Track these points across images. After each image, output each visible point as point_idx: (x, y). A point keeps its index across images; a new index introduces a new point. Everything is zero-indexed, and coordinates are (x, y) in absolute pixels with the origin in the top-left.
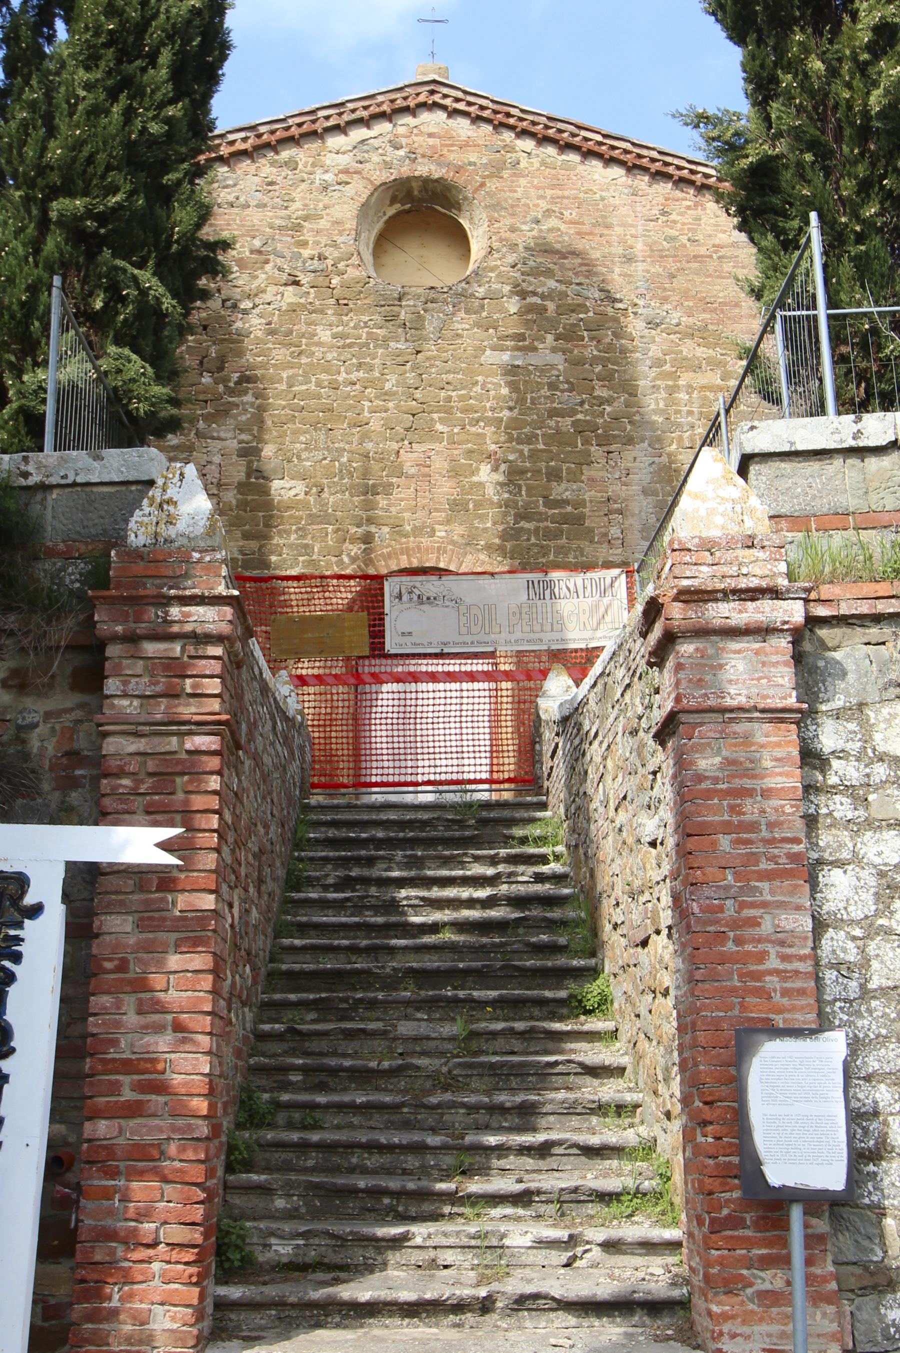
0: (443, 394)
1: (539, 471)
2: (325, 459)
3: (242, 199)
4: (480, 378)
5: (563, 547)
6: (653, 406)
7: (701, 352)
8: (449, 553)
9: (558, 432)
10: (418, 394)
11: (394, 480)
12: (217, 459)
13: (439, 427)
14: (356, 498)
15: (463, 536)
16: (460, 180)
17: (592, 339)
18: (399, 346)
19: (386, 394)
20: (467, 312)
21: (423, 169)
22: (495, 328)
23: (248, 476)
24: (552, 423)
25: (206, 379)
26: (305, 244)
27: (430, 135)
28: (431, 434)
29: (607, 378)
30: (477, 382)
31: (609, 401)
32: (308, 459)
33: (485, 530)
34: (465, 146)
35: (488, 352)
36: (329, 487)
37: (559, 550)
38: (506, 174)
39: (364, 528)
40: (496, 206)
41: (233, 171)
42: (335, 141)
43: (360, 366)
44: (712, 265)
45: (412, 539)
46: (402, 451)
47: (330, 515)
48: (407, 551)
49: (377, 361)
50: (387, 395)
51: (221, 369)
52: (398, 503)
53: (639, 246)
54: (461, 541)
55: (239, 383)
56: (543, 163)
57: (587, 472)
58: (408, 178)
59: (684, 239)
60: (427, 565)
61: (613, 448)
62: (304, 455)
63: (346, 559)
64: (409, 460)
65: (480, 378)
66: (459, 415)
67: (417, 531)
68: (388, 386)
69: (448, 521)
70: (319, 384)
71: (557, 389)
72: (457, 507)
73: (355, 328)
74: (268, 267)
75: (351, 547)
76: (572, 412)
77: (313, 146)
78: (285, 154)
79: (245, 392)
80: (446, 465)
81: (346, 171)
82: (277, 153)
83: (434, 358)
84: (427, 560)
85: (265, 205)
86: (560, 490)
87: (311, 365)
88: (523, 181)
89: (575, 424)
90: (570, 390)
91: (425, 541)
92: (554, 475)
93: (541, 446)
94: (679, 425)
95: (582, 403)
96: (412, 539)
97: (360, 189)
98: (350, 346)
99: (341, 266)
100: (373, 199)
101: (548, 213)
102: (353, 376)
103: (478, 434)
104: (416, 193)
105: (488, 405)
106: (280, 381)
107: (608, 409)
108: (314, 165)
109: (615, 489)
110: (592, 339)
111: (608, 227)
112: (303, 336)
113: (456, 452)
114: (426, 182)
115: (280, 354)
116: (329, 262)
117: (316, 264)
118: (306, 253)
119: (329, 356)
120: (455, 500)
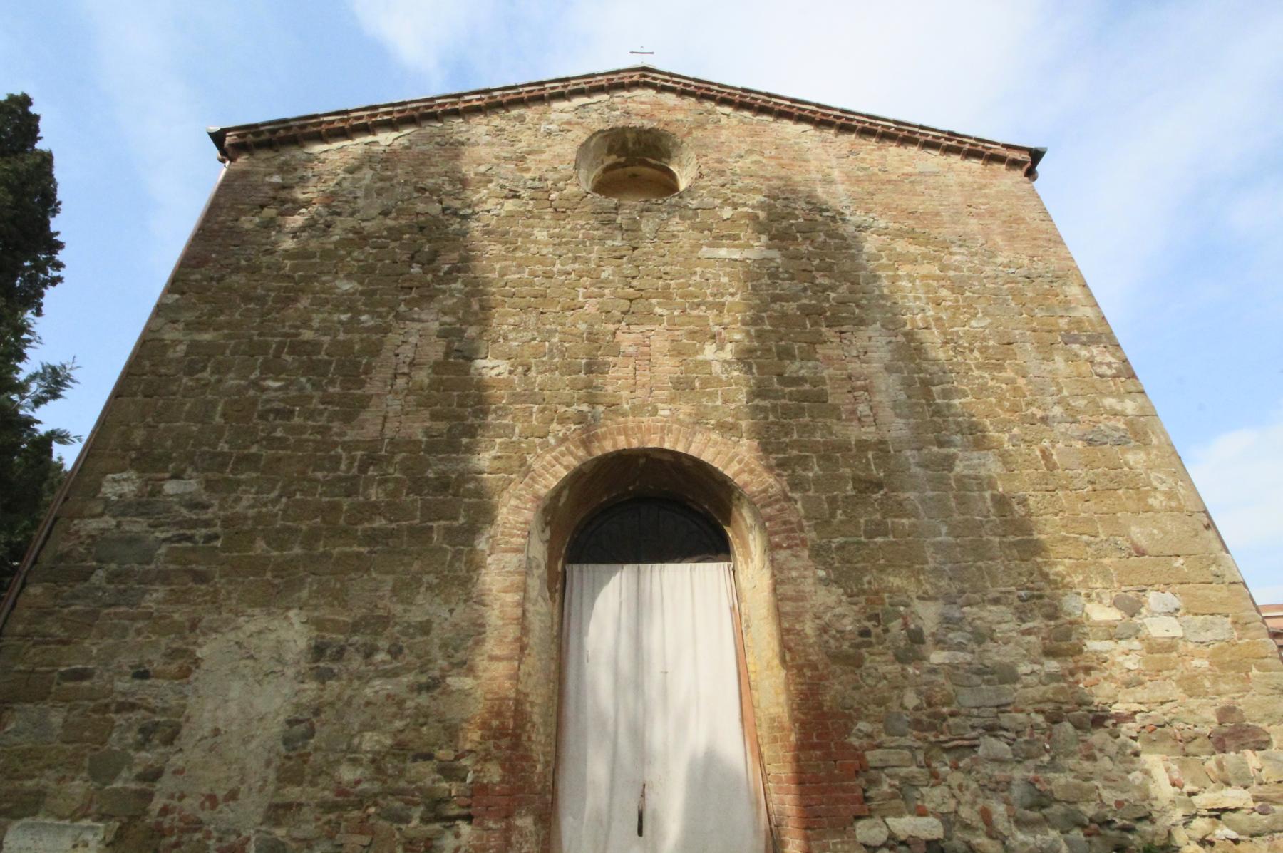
0: (661, 283)
1: (769, 350)
2: (534, 339)
3: (472, 140)
4: (698, 269)
5: (807, 425)
6: (877, 292)
7: (913, 249)
8: (675, 432)
9: (784, 315)
10: (635, 283)
11: (611, 359)
13: (658, 310)
14: (566, 377)
15: (690, 415)
16: (671, 129)
17: (805, 239)
18: (616, 243)
19: (602, 282)
20: (682, 218)
21: (636, 122)
22: (710, 230)
23: (447, 355)
24: (777, 306)
25: (416, 269)
26: (528, 170)
27: (642, 103)
28: (650, 316)
29: (827, 269)
30: (695, 273)
31: (832, 288)
32: (515, 340)
33: (715, 408)
34: (674, 108)
35: (705, 248)
36: (537, 366)
37: (803, 428)
38: (709, 127)
39: (575, 407)
40: (704, 146)
41: (467, 122)
42: (557, 105)
43: (575, 259)
44: (906, 187)
45: (631, 418)
46: (618, 332)
47: (536, 394)
48: (624, 431)
50: (601, 284)
51: (431, 261)
52: (617, 380)
53: (836, 174)
54: (688, 420)
55: (449, 273)
56: (741, 121)
57: (821, 351)
58: (623, 128)
59: (875, 170)
60: (650, 446)
61: (845, 328)
62: (511, 336)
63: (552, 440)
64: (627, 340)
65: (698, 269)
66: (678, 300)
67: (636, 410)
68: (604, 275)
69: (672, 400)
71: (778, 278)
72: (682, 386)
73: (571, 229)
74: (490, 185)
75: (559, 427)
76: (794, 298)
77: (540, 108)
78: (515, 112)
80: (667, 344)
81: (569, 123)
82: (508, 111)
83: (652, 253)
84: (650, 441)
85: (493, 144)
86: (794, 368)
87: (526, 258)
88: (724, 132)
89: (799, 308)
90: (792, 279)
92: (786, 354)
94: (908, 309)
95: (805, 289)
96: (631, 418)
97: (580, 135)
98: (566, 243)
99: (561, 184)
100: (592, 144)
101: (750, 152)
102: (569, 268)
103: (700, 317)
104: (630, 145)
105: (708, 292)
106: (493, 270)
107: (832, 295)
110: (805, 239)
111: (807, 161)
112: (520, 235)
113: (677, 333)
114: (640, 132)
115: (496, 249)
116: (549, 183)
117: (537, 184)
119: (544, 251)
120: (678, 378)
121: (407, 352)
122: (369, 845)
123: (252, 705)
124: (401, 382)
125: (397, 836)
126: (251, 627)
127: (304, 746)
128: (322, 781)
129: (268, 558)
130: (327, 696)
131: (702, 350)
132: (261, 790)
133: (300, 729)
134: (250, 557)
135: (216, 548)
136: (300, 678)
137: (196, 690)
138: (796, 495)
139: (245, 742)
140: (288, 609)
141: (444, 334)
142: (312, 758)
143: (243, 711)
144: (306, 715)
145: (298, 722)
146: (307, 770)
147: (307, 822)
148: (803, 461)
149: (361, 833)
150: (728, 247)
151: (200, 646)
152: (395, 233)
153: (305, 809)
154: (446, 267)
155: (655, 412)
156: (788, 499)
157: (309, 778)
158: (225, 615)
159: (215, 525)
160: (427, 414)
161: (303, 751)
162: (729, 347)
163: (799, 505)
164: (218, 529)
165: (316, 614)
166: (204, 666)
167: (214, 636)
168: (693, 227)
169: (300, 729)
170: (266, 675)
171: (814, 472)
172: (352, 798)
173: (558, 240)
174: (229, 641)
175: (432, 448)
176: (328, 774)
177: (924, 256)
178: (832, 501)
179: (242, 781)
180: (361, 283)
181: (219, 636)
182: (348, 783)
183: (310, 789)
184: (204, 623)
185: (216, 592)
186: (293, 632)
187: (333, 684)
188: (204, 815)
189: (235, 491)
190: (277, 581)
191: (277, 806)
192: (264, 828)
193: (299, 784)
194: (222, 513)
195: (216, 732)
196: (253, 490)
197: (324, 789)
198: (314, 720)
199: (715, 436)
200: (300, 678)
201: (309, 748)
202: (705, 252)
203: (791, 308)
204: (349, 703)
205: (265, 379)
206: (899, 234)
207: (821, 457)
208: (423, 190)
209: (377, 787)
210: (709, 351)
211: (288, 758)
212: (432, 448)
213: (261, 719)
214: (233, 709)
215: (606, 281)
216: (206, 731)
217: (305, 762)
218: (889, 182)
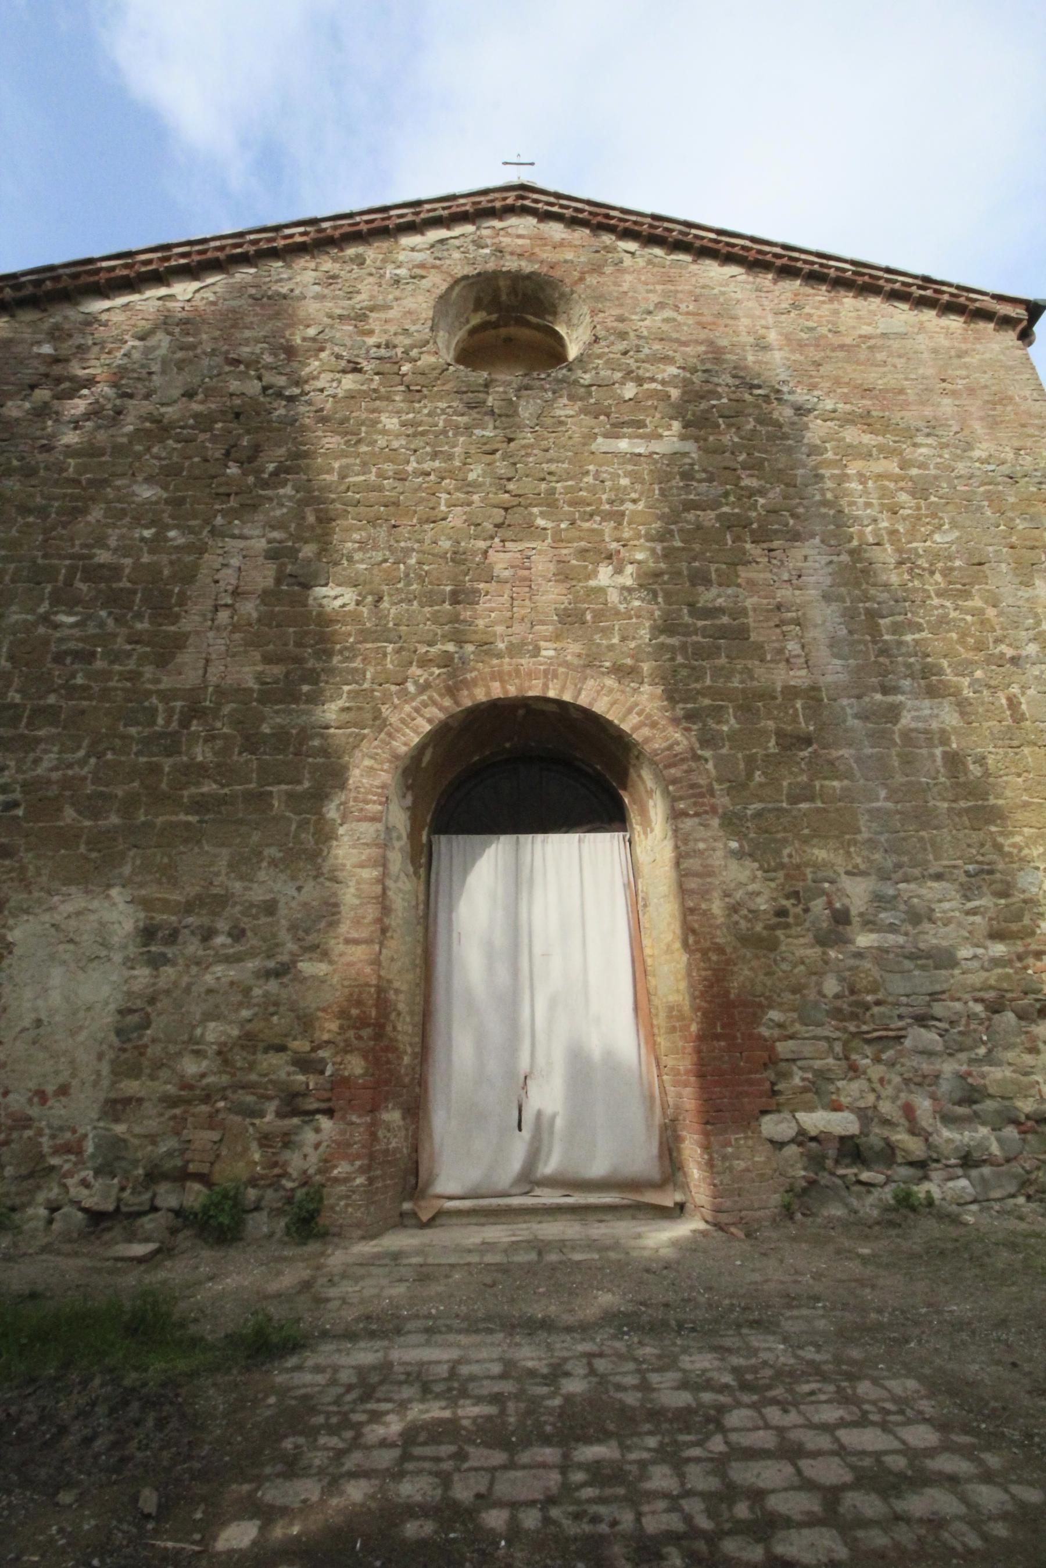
0: (543, 486)
1: (679, 573)
2: (385, 561)
3: (297, 292)
4: (591, 467)
5: (722, 668)
6: (818, 498)
7: (867, 439)
8: (562, 677)
9: (699, 527)
10: (511, 486)
11: (482, 586)
12: (235, 562)
13: (541, 522)
14: (427, 609)
15: (579, 656)
16: (557, 273)
17: (729, 426)
18: (487, 433)
19: (469, 485)
20: (571, 397)
21: (511, 264)
22: (608, 415)
23: (278, 581)
24: (691, 516)
25: (233, 470)
26: (371, 333)
27: (519, 236)
28: (530, 530)
29: (755, 466)
30: (587, 472)
31: (761, 492)
32: (362, 561)
33: (611, 648)
34: (561, 244)
35: (600, 440)
36: (390, 595)
37: (717, 672)
38: (608, 270)
39: (439, 646)
40: (600, 298)
41: (289, 266)
43: (435, 455)
45: (507, 660)
46: (491, 552)
47: (389, 630)
48: (499, 676)
49: (457, 450)
50: (470, 487)
51: (251, 459)
52: (489, 612)
53: (772, 336)
54: (576, 661)
55: (275, 473)
56: (649, 262)
57: (744, 573)
58: (494, 272)
59: (824, 330)
60: (530, 694)
61: (776, 544)
62: (357, 556)
63: (411, 688)
64: (501, 562)
65: (591, 467)
66: (566, 508)
67: (514, 650)
68: (472, 476)
69: (557, 637)
70: (381, 475)
71: (693, 479)
72: (570, 619)
73: (429, 415)
74: (323, 355)
75: (419, 672)
76: (715, 505)
77: (385, 245)
78: (351, 251)
79: (284, 484)
80: (552, 567)
81: (422, 266)
82: (342, 250)
83: (531, 446)
84: (530, 688)
85: (324, 297)
86: (710, 596)
87: (373, 454)
88: (628, 277)
89: (719, 518)
90: (710, 480)
91: (526, 662)
92: (700, 579)
93: (678, 544)
94: (856, 519)
95: (726, 494)
96: (507, 660)
97: (437, 283)
98: (423, 434)
99: (414, 353)
100: (454, 294)
101: (661, 306)
102: (427, 466)
103: (593, 530)
104: (504, 297)
105: (604, 497)
106: (330, 471)
107: (762, 501)
108: (384, 261)
109: (784, 594)
110: (729, 426)
111: (734, 318)
112: (363, 424)
113: (564, 551)
114: (516, 278)
115: (332, 442)
116: (399, 351)
117: (383, 352)
118: (371, 341)
119: (395, 444)
120: (565, 609)
121: (228, 577)
122: (221, 1140)
123: (76, 994)
124: (223, 616)
125: (251, 1130)
126: (69, 908)
127: (140, 1037)
128: (164, 1074)
129: (82, 829)
130: (162, 983)
131: (595, 573)
132: (95, 1084)
133: (133, 1019)
134: (61, 828)
135: (18, 817)
136: (129, 963)
137: (11, 978)
138: (707, 753)
139: (73, 1033)
140: (109, 886)
141: (273, 555)
142: (149, 1050)
143: (67, 999)
144: (139, 1003)
145: (130, 1011)
146: (146, 1063)
147: (150, 1117)
148: (717, 712)
149: (211, 1128)
150: (630, 437)
151: (11, 929)
152: (204, 422)
153: (146, 1104)
154: (271, 467)
155: (536, 652)
156: (696, 758)
157: (148, 1071)
158: (36, 894)
159: (14, 791)
160: (257, 656)
161: (140, 1043)
162: (630, 569)
163: (710, 766)
164: (17, 795)
165: (143, 892)
166: (18, 951)
167: (25, 917)
168: (584, 411)
169: (133, 1019)
170: (91, 960)
171: (729, 724)
172: (198, 1092)
173: (413, 429)
174: (44, 923)
175: (266, 697)
176: (169, 1067)
177: (881, 448)
178: (750, 760)
179: (73, 1075)
180: (165, 488)
181: (31, 918)
182: (193, 1076)
183: (149, 1083)
184: (12, 904)
185: (23, 869)
186: (117, 913)
187: (168, 971)
188: (34, 1111)
189: (33, 750)
190: (94, 855)
191: (115, 1101)
192: (101, 1124)
193: (137, 1077)
194: (20, 777)
195: (39, 1023)
196: (56, 749)
197: (166, 1083)
198: (149, 1009)
199: (610, 682)
200: (129, 964)
201: (145, 1039)
202: (601, 444)
203: (708, 518)
204: (188, 990)
205: (57, 613)
206: (849, 420)
207: (739, 707)
208: (237, 362)
209: (225, 1079)
210: (604, 576)
211: (124, 1050)
212: (266, 697)
213: (89, 1009)
214: (56, 998)
215: (475, 485)
216: (27, 1022)
217: (142, 1054)
218: (842, 347)
